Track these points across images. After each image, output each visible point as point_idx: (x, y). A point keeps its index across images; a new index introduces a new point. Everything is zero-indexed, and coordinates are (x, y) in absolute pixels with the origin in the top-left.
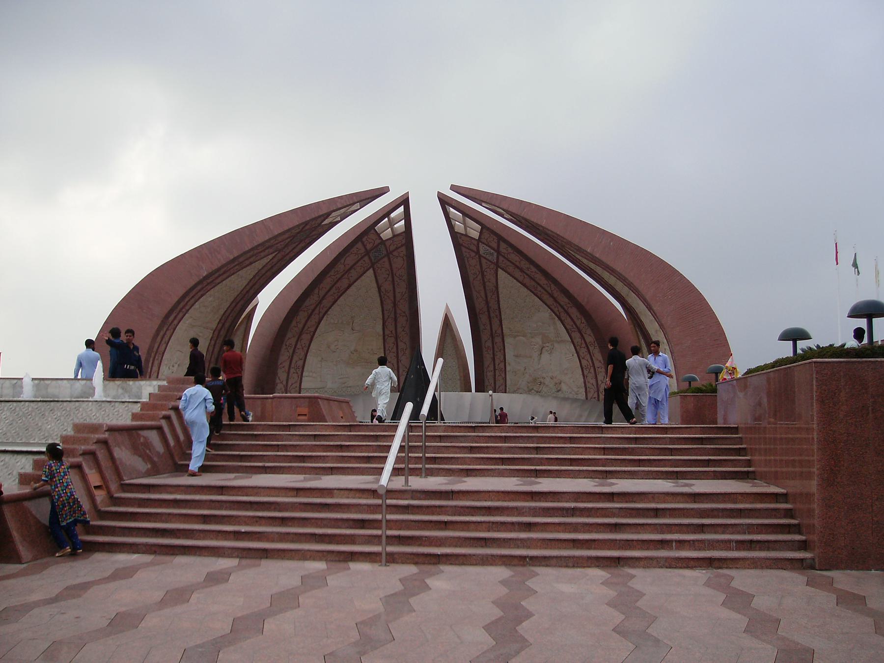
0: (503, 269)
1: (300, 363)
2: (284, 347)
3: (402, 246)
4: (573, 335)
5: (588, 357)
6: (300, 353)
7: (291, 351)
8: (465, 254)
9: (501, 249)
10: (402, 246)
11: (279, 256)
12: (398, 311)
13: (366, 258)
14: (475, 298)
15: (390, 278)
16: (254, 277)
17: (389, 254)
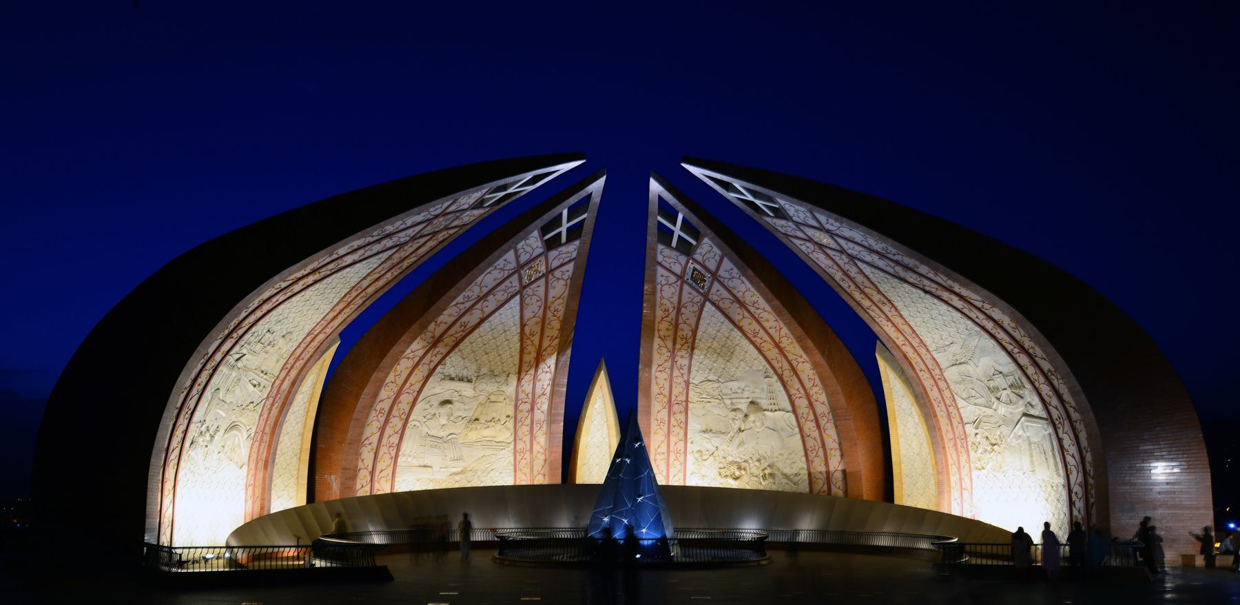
0: (714, 304)
1: (395, 440)
2: (373, 413)
3: (570, 261)
4: (797, 402)
5: (816, 434)
6: (396, 423)
7: (382, 420)
8: (659, 279)
9: (721, 272)
10: (570, 261)
11: (396, 258)
12: (542, 366)
13: (515, 278)
14: (656, 346)
15: (540, 313)
16: (349, 292)
17: (550, 271)
